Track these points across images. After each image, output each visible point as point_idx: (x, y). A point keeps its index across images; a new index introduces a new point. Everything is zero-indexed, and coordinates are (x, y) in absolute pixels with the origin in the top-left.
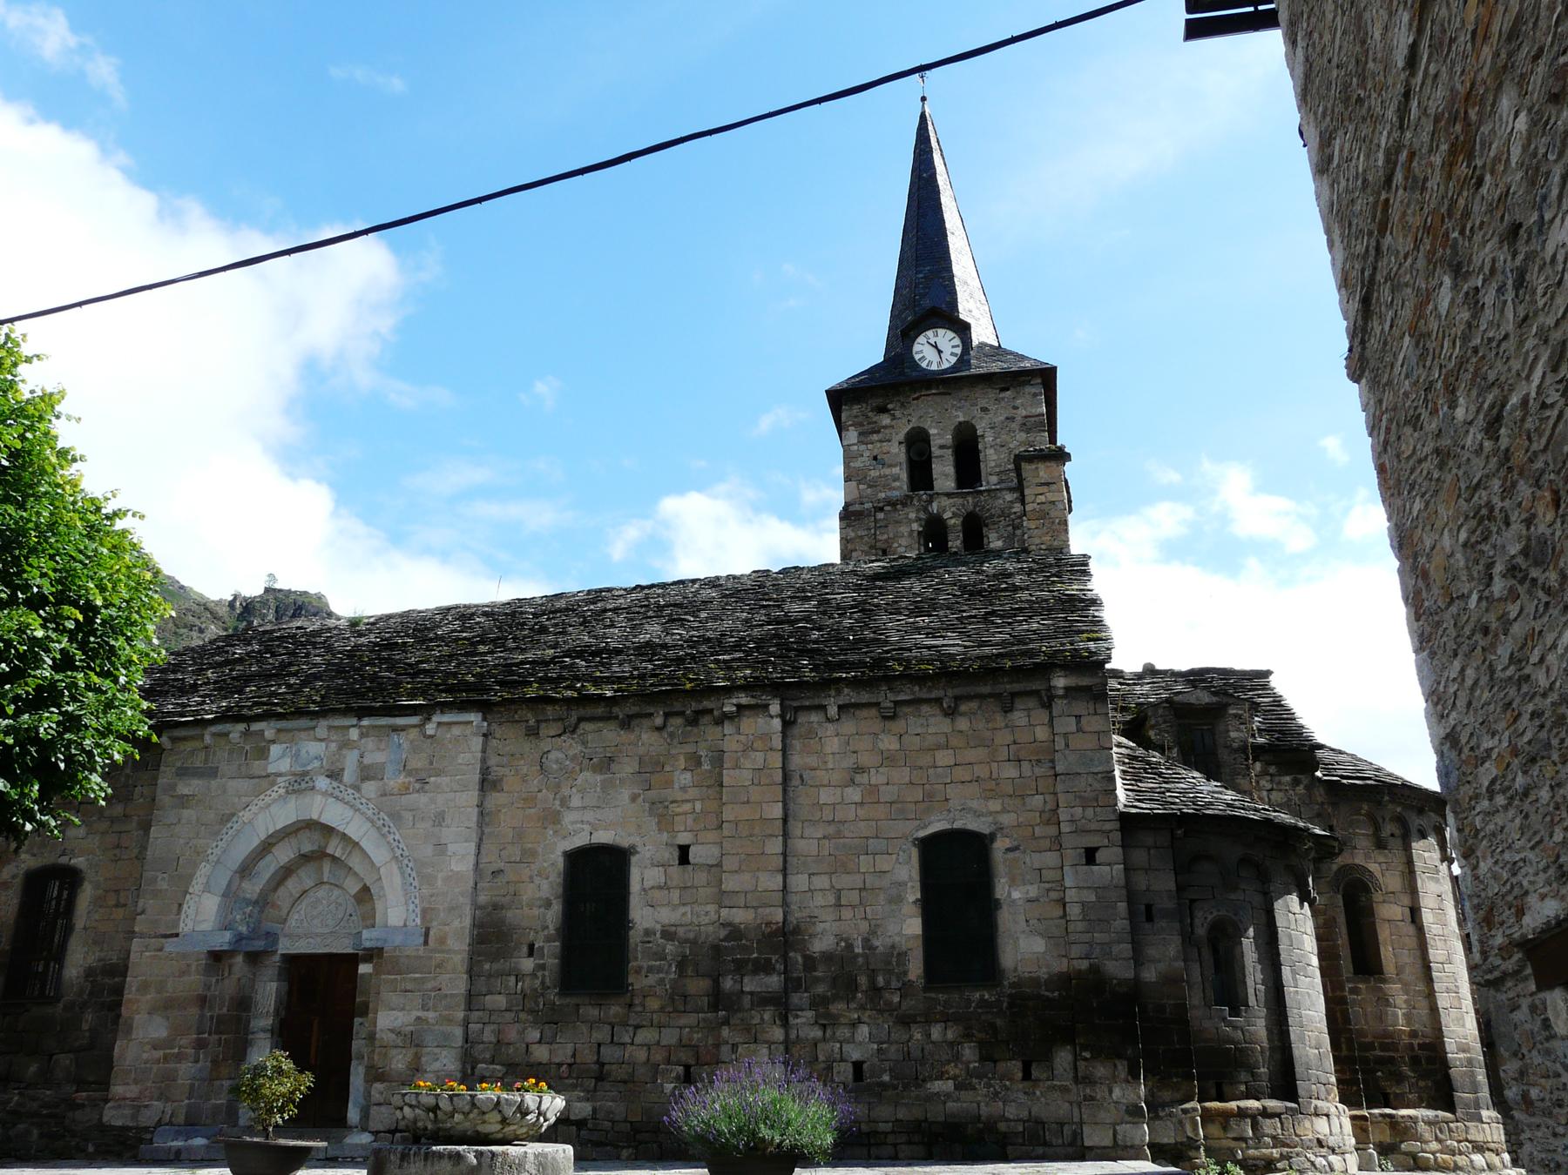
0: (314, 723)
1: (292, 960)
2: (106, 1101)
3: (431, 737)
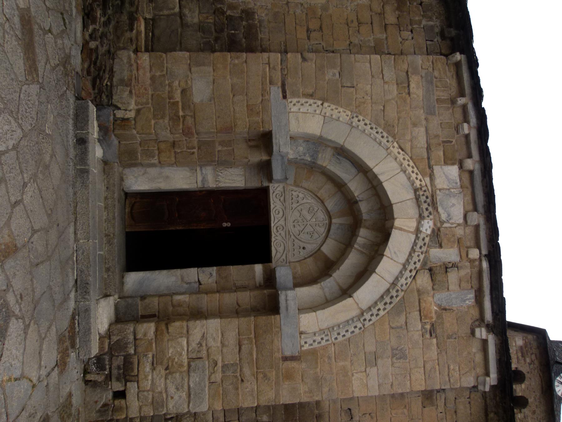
0: (481, 209)
2: (136, 51)
3: (473, 333)
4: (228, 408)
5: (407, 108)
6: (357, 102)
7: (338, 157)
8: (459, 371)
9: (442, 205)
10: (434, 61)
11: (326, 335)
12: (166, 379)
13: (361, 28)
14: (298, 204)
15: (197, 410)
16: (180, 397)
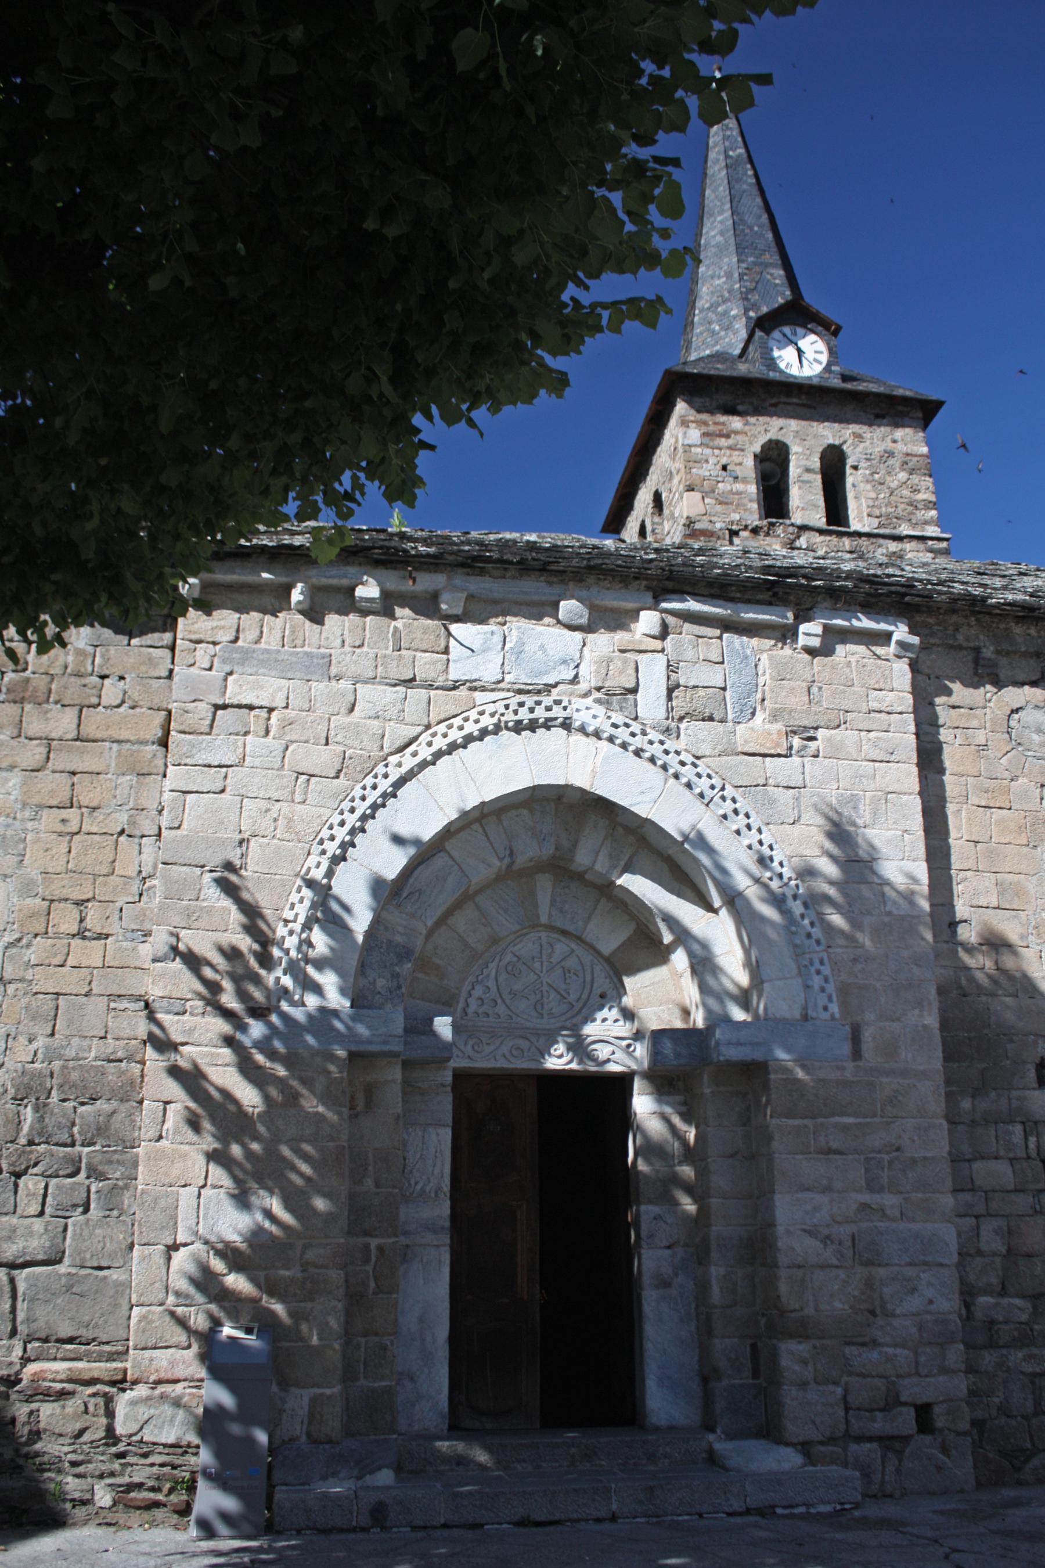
1: (459, 1076)
2: (121, 1383)
4: (951, 1183)
5: (309, 719)
6: (287, 836)
7: (405, 895)
8: (881, 690)
9: (542, 674)
10: (194, 637)
11: (812, 963)
12: (894, 1315)
13: (84, 803)
14: (499, 1001)
15: (954, 1248)
16: (929, 1284)
